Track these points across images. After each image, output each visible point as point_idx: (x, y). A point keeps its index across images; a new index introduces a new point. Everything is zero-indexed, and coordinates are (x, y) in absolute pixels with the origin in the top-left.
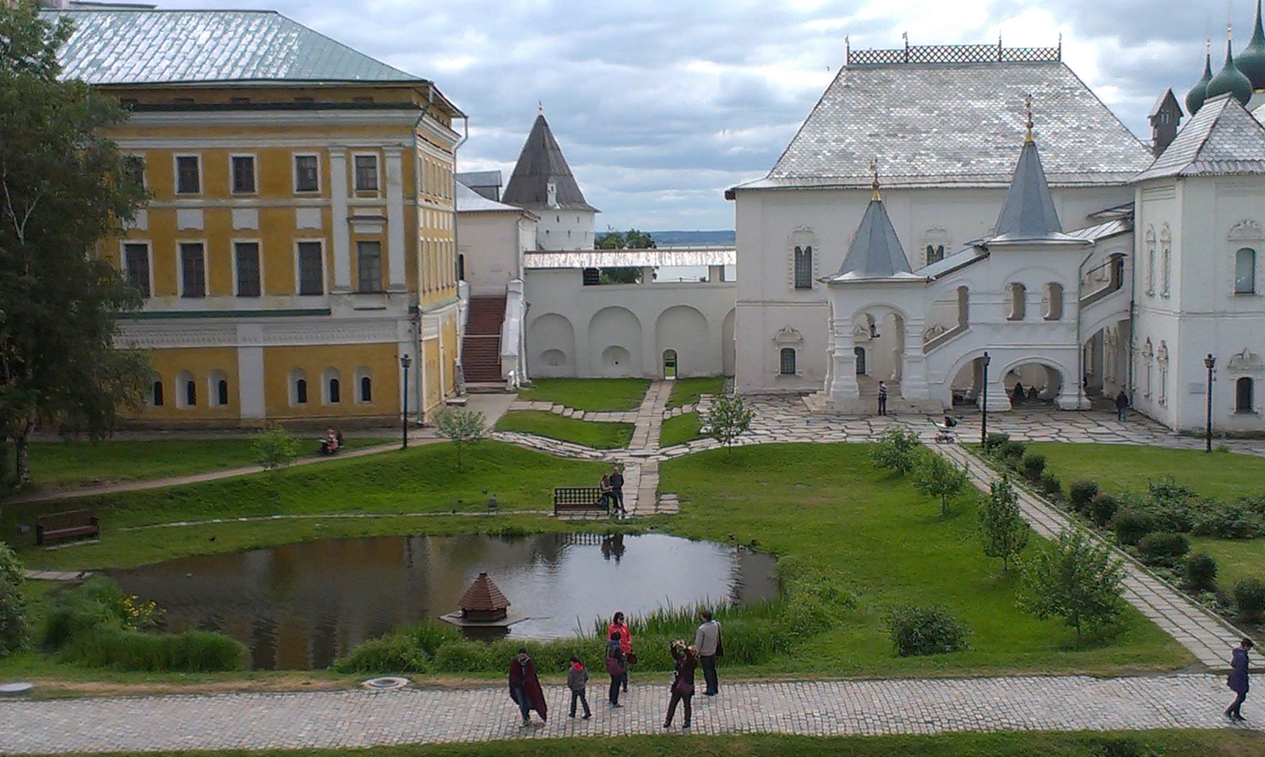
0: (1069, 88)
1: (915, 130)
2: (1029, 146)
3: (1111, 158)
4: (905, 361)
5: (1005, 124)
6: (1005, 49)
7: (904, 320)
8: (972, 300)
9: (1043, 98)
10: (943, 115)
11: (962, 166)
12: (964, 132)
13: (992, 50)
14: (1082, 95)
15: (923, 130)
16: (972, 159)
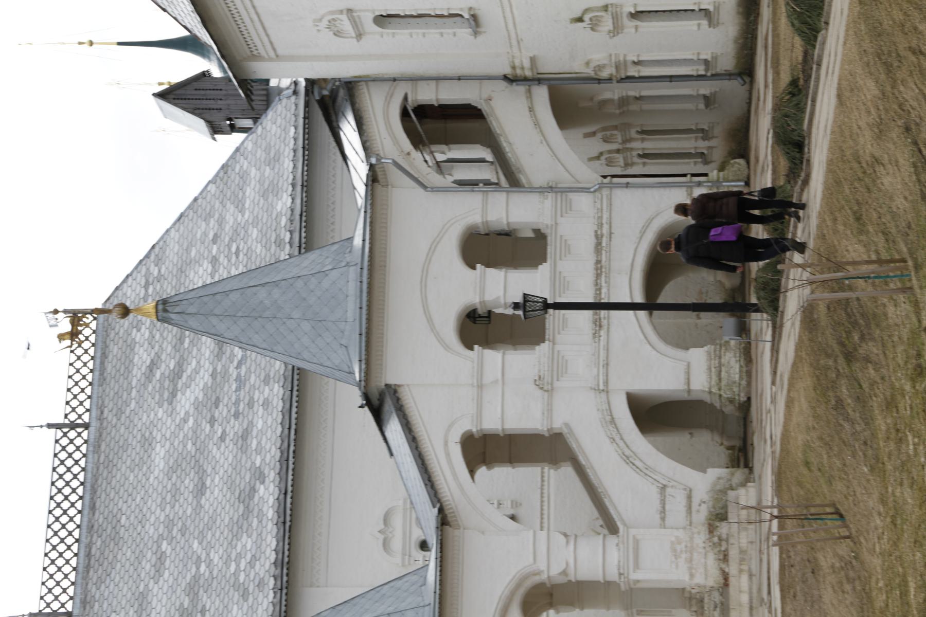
0: (146, 287)
1: (192, 590)
2: (165, 311)
3: (269, 191)
4: (634, 576)
5: (197, 405)
6: (66, 416)
7: (537, 579)
8: (492, 423)
9: (158, 336)
10: (170, 532)
11: (263, 483)
12: (204, 484)
13: (65, 441)
14: (158, 262)
15: (194, 570)
16: (253, 463)
